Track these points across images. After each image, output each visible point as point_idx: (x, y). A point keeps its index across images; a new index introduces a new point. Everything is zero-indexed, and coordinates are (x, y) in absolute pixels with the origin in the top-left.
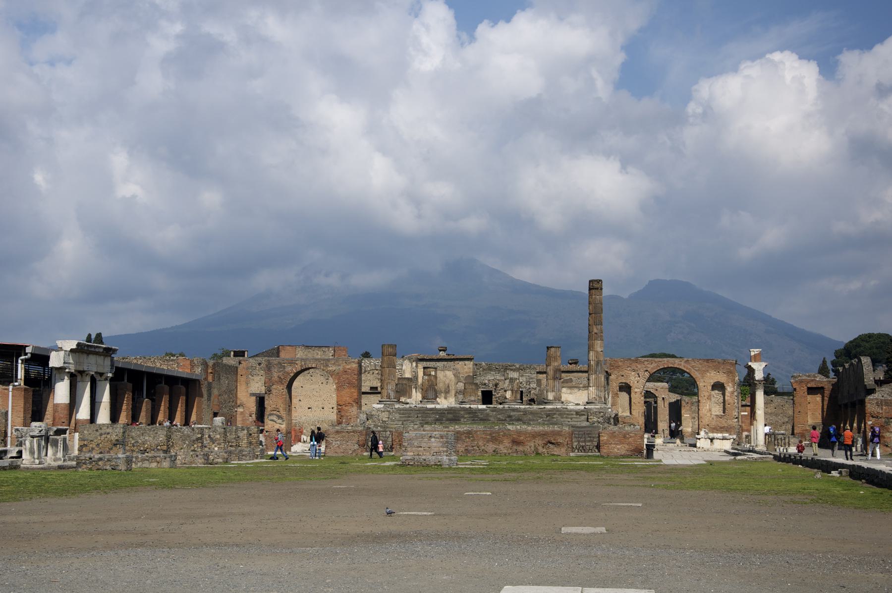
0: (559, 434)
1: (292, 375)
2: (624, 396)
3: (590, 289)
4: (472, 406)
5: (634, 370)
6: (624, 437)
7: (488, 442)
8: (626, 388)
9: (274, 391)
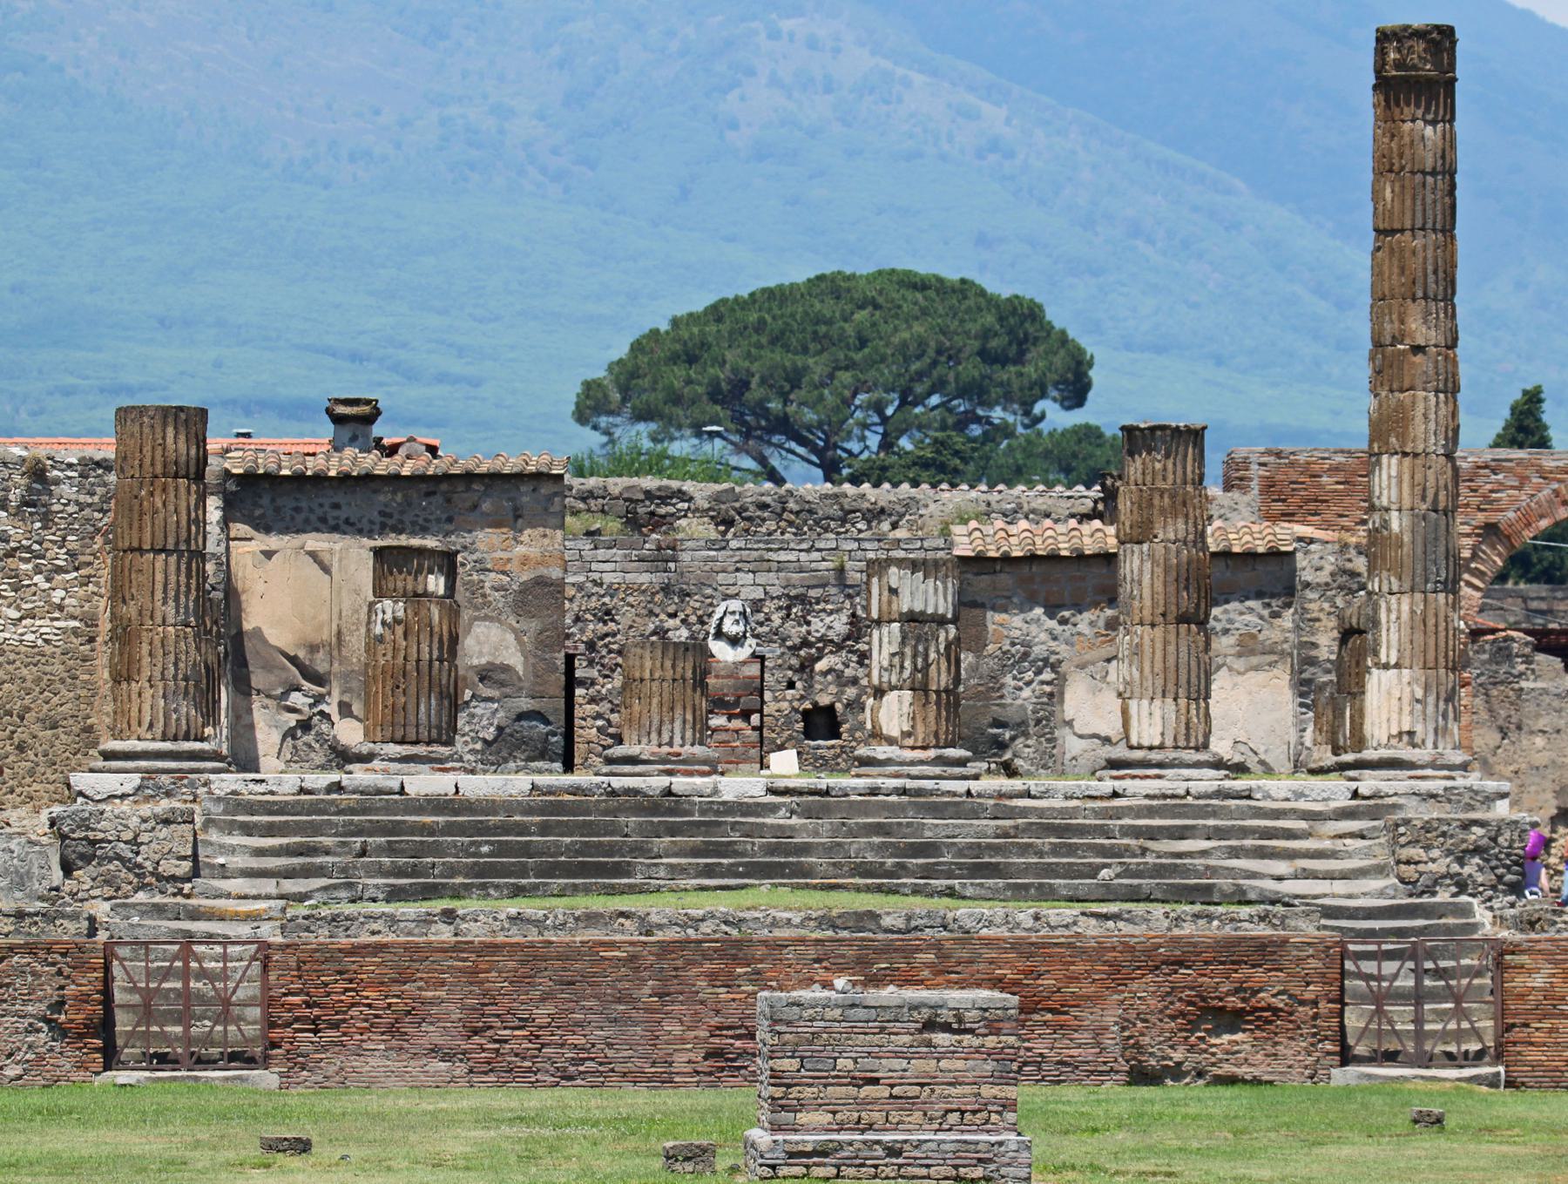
0: (1264, 952)
4: (680, 783)
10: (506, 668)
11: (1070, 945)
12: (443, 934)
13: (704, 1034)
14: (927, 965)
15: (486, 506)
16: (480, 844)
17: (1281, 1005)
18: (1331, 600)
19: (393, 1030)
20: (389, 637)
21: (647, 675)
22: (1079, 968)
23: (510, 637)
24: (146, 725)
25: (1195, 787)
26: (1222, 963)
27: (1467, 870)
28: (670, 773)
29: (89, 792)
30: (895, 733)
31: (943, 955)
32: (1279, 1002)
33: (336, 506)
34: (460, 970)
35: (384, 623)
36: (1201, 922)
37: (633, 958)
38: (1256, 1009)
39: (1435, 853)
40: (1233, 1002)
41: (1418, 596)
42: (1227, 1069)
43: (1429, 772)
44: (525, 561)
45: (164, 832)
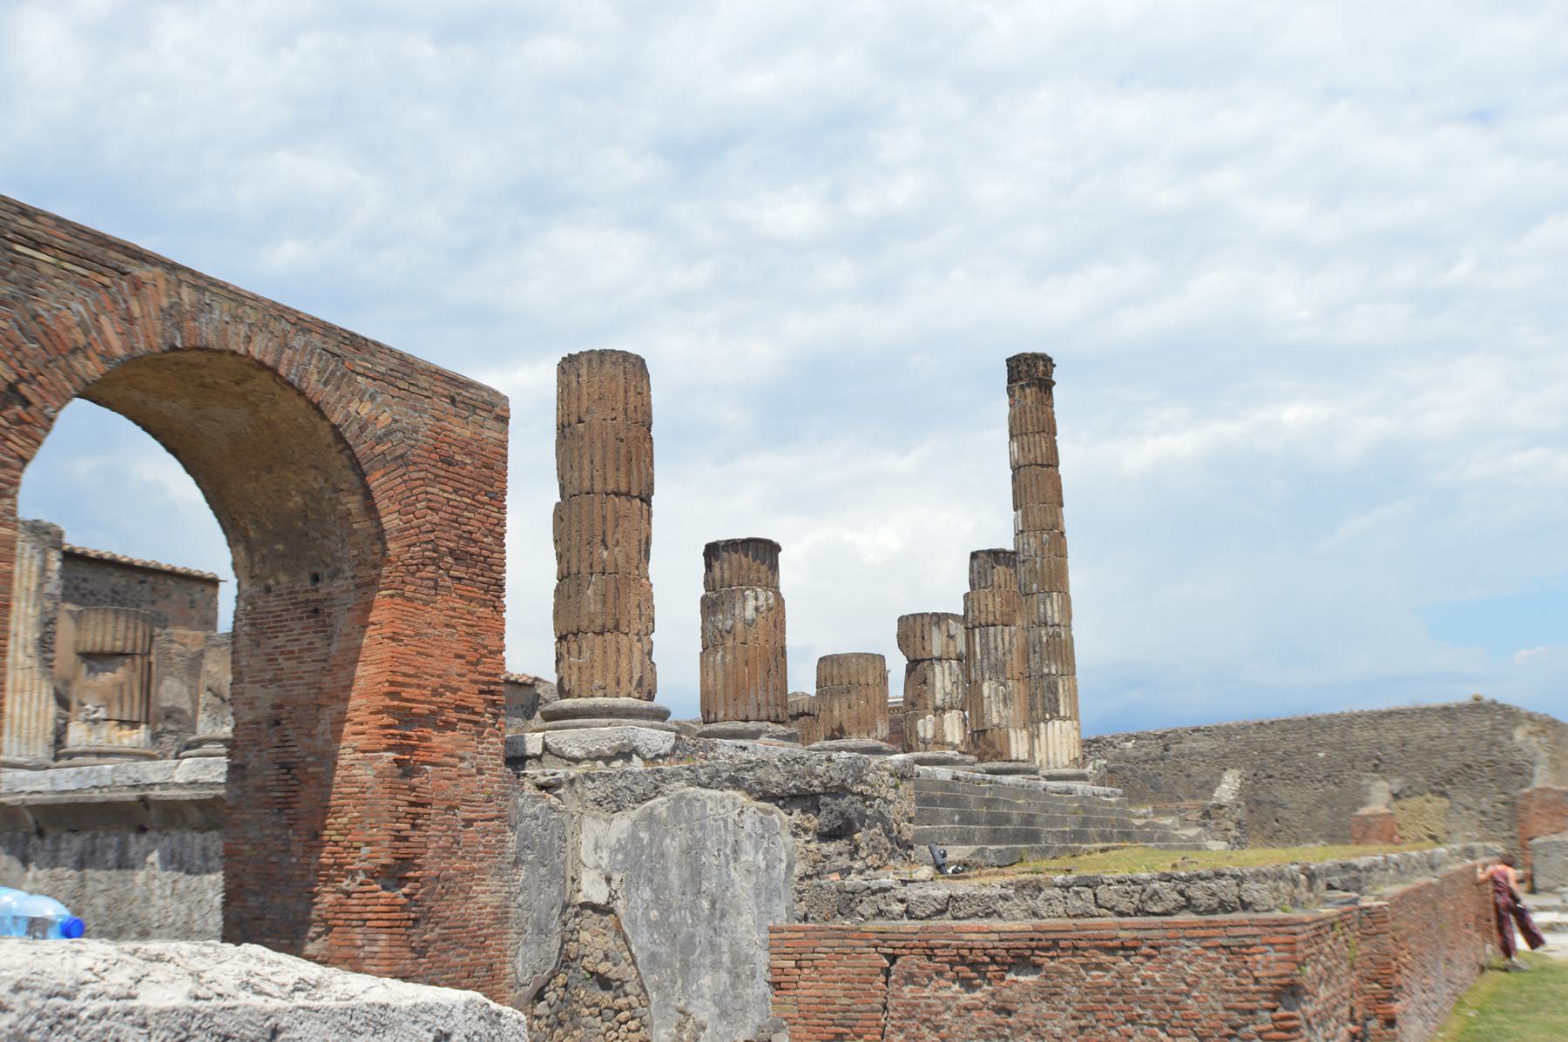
10: (182, 712)
15: (175, 597)
16: (953, 813)
20: (761, 622)
21: (871, 681)
23: (185, 689)
24: (635, 682)
29: (643, 750)
30: (957, 741)
33: (85, 580)
35: (757, 609)
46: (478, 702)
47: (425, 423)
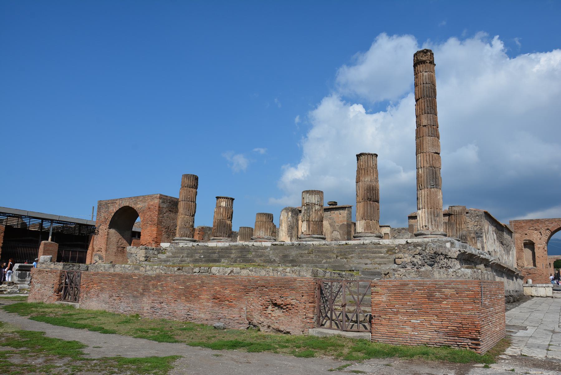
1: (113, 214)
2: (528, 252)
3: (415, 66)
4: (255, 244)
5: (536, 230)
6: (430, 297)
7: (179, 296)
8: (530, 245)
9: (100, 231)
11: (234, 279)
12: (112, 270)
13: (150, 302)
14: (200, 284)
17: (294, 303)
18: (471, 219)
19: (98, 296)
22: (236, 287)
25: (366, 242)
26: (276, 287)
27: (415, 260)
28: (256, 241)
31: (203, 282)
32: (293, 302)
34: (110, 280)
36: (275, 272)
37: (138, 279)
38: (288, 304)
39: (406, 255)
40: (279, 302)
41: (426, 189)
42: (276, 326)
43: (430, 236)
44: (341, 221)
45: (141, 251)
46: (152, 242)
47: (146, 204)
